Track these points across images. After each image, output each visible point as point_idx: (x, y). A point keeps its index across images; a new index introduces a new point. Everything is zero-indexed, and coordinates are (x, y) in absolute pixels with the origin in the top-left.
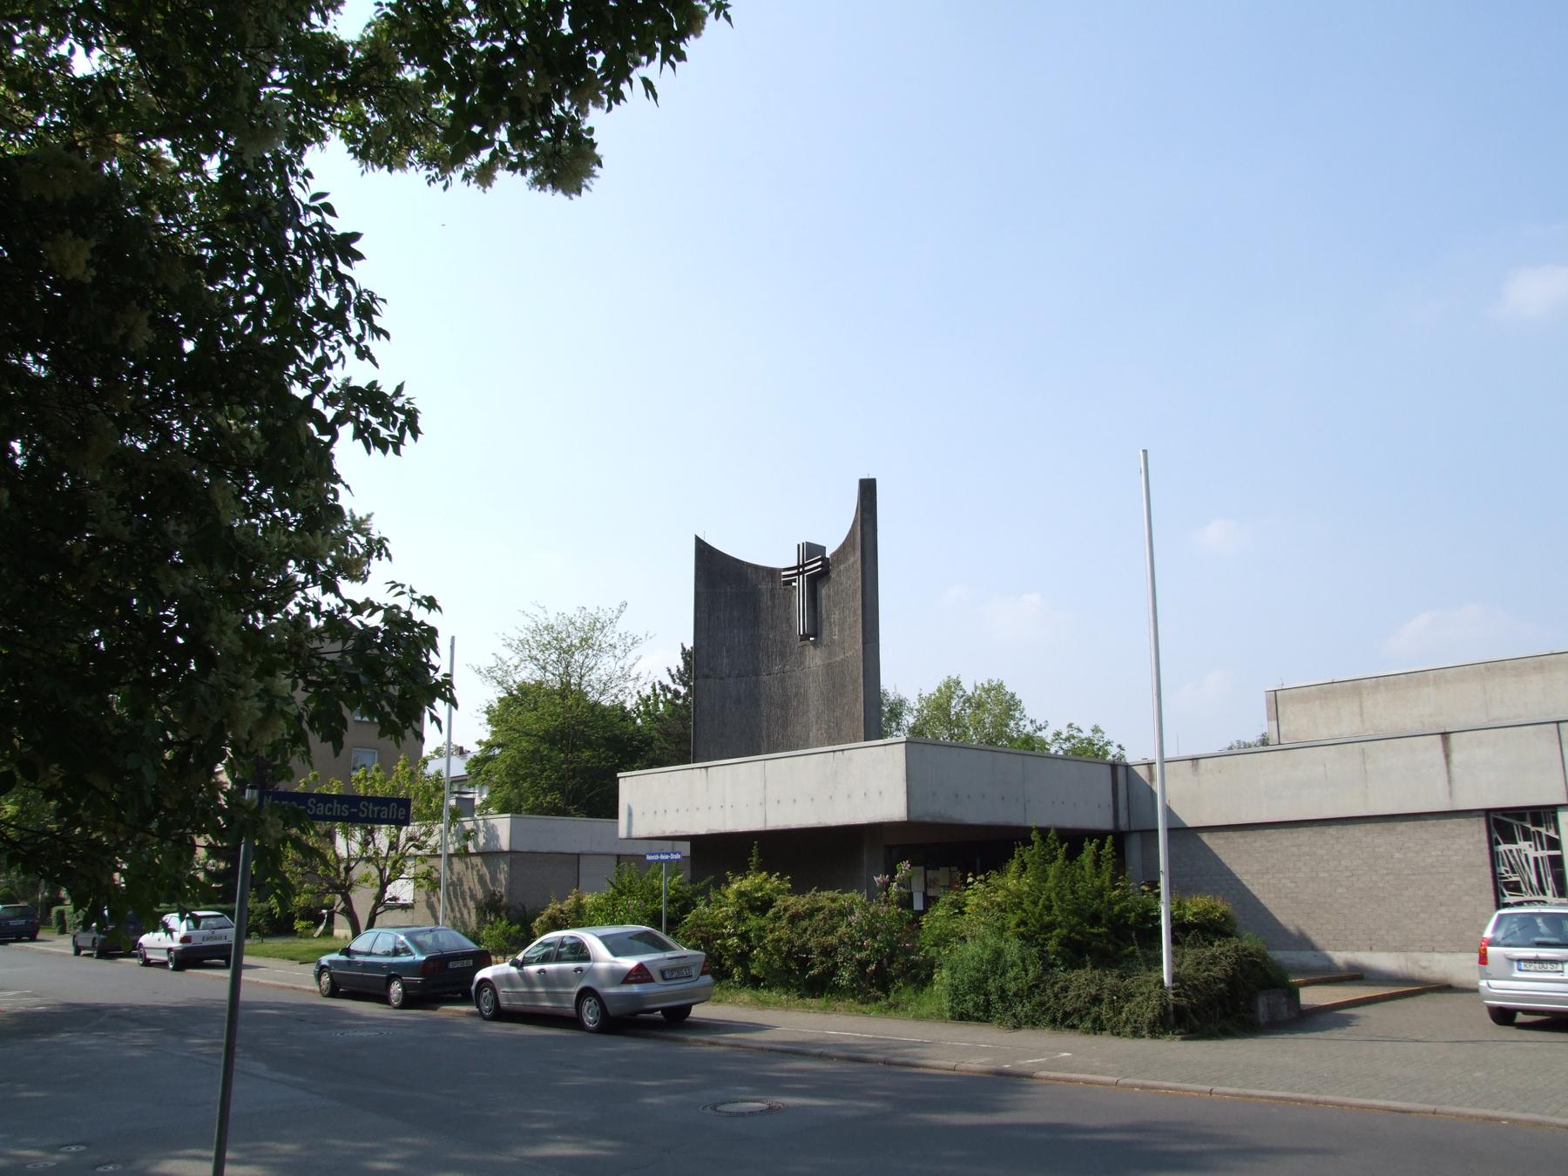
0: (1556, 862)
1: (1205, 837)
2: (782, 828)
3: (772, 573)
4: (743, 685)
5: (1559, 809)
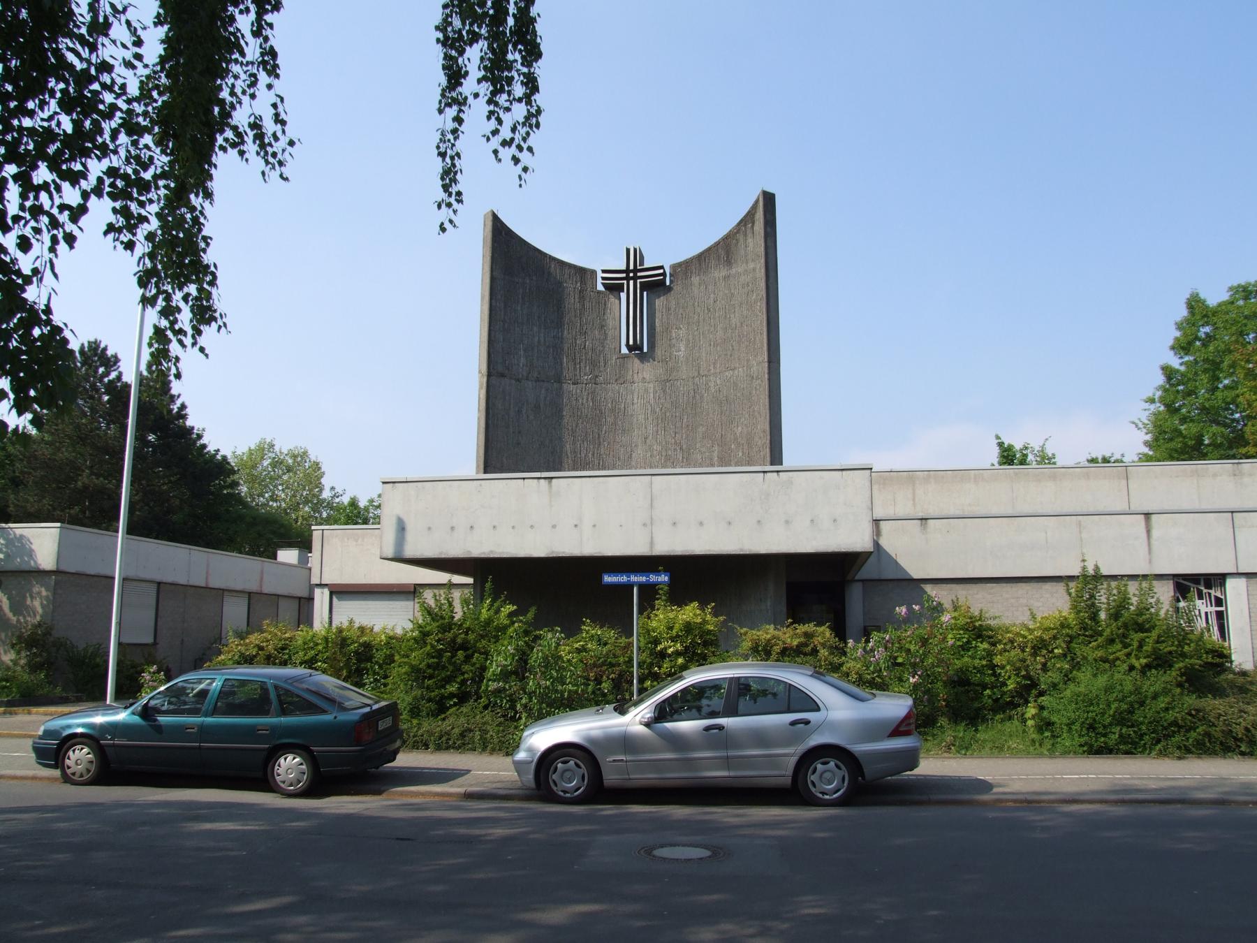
0: (1220, 616)
1: (928, 588)
2: (680, 553)
3: (584, 274)
4: (543, 391)
5: (1228, 576)
